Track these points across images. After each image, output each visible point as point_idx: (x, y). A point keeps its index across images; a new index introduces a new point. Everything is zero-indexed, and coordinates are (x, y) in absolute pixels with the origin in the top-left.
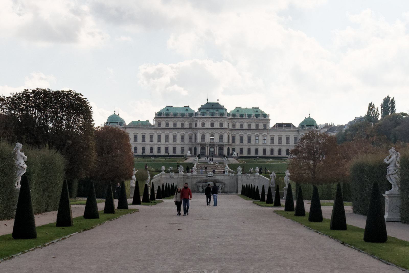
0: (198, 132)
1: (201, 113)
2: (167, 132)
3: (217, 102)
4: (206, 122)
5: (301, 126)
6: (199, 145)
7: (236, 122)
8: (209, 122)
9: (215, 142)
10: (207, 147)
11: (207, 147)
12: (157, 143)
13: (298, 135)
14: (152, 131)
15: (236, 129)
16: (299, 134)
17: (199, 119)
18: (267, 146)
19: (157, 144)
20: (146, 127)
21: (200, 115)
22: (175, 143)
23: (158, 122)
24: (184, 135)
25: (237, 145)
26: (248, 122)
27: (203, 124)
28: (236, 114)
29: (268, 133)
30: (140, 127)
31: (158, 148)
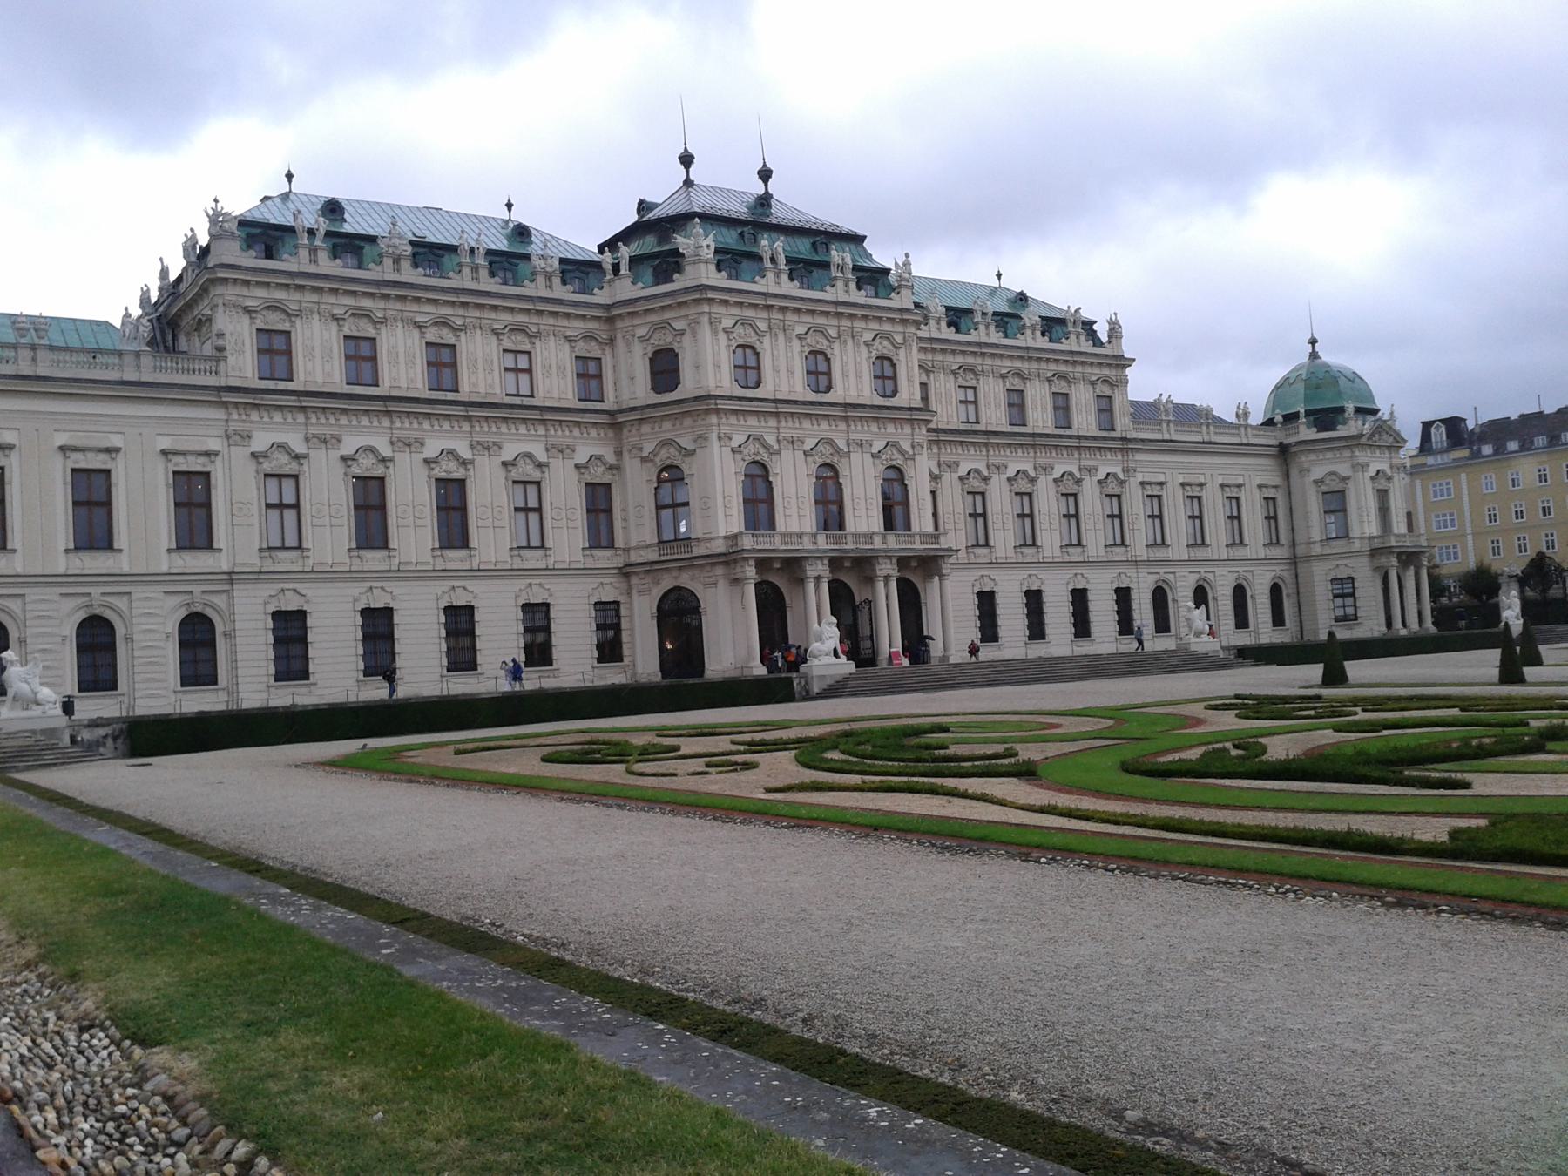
0: (702, 439)
2: (362, 436)
3: (759, 189)
6: (750, 571)
9: (869, 537)
12: (268, 566)
13: (1277, 481)
14: (197, 431)
17: (706, 308)
18: (1136, 563)
19: (259, 576)
20: (113, 375)
22: (455, 558)
23: (259, 324)
26: (1003, 377)
27: (749, 368)
29: (1132, 464)
30: (42, 371)
31: (277, 615)
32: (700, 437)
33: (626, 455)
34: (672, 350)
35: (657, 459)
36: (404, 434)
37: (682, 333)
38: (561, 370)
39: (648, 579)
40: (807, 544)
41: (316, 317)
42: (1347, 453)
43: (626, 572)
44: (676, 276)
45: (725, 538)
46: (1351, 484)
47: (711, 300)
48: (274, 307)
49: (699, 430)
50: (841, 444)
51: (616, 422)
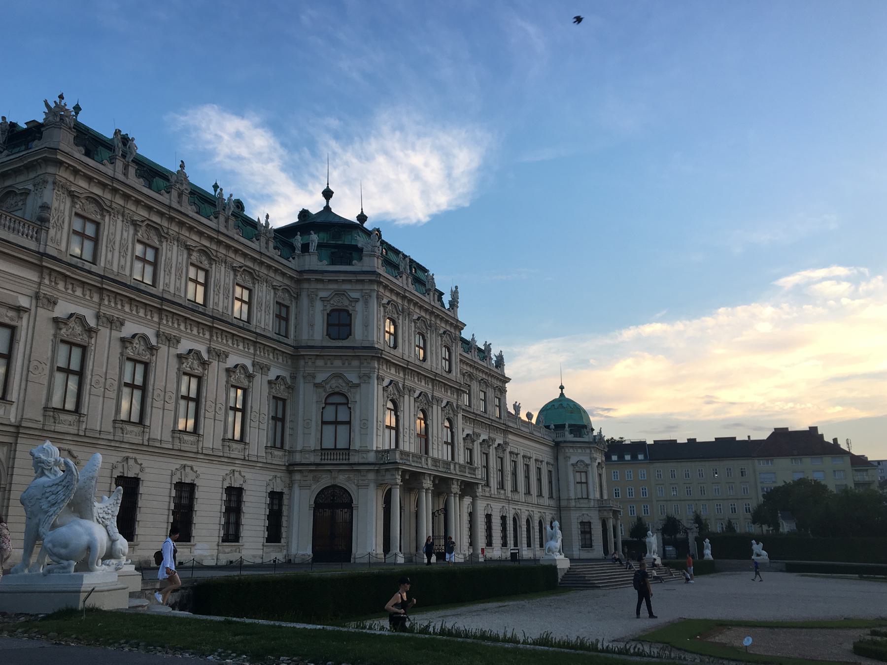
5: (570, 426)
13: (552, 461)
16: (556, 459)
32: (365, 375)
33: (301, 381)
34: (347, 311)
36: (168, 331)
37: (357, 300)
38: (268, 306)
39: (310, 476)
41: (120, 218)
42: (588, 451)
43: (291, 469)
45: (377, 452)
46: (590, 469)
47: (380, 283)
48: (94, 200)
49: (364, 371)
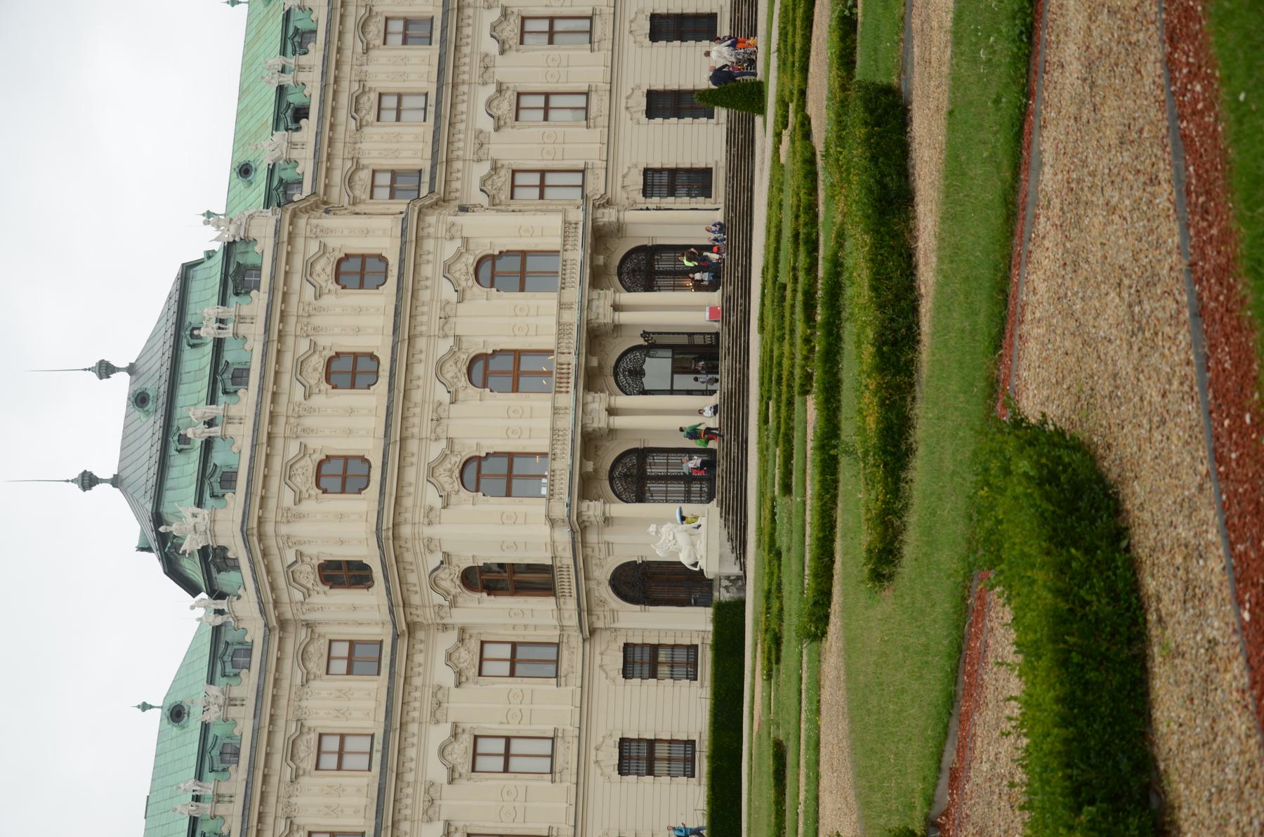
0: (429, 544)
1: (200, 503)
4: (314, 443)
6: (593, 509)
7: (358, 167)
8: (311, 410)
10: (612, 412)
11: (612, 412)
15: (427, 167)
17: (269, 528)
21: (220, 514)
24: (466, 740)
25: (610, 144)
26: (367, 50)
27: (341, 474)
28: (271, 171)
35: (453, 591)
37: (300, 554)
39: (598, 610)
40: (567, 422)
44: (230, 555)
47: (261, 521)
49: (419, 547)
50: (444, 346)
51: (407, 630)
